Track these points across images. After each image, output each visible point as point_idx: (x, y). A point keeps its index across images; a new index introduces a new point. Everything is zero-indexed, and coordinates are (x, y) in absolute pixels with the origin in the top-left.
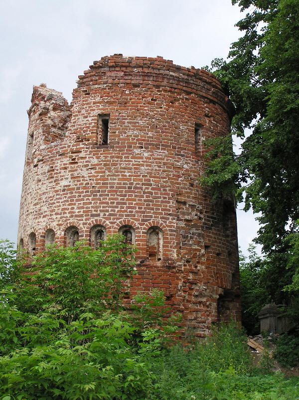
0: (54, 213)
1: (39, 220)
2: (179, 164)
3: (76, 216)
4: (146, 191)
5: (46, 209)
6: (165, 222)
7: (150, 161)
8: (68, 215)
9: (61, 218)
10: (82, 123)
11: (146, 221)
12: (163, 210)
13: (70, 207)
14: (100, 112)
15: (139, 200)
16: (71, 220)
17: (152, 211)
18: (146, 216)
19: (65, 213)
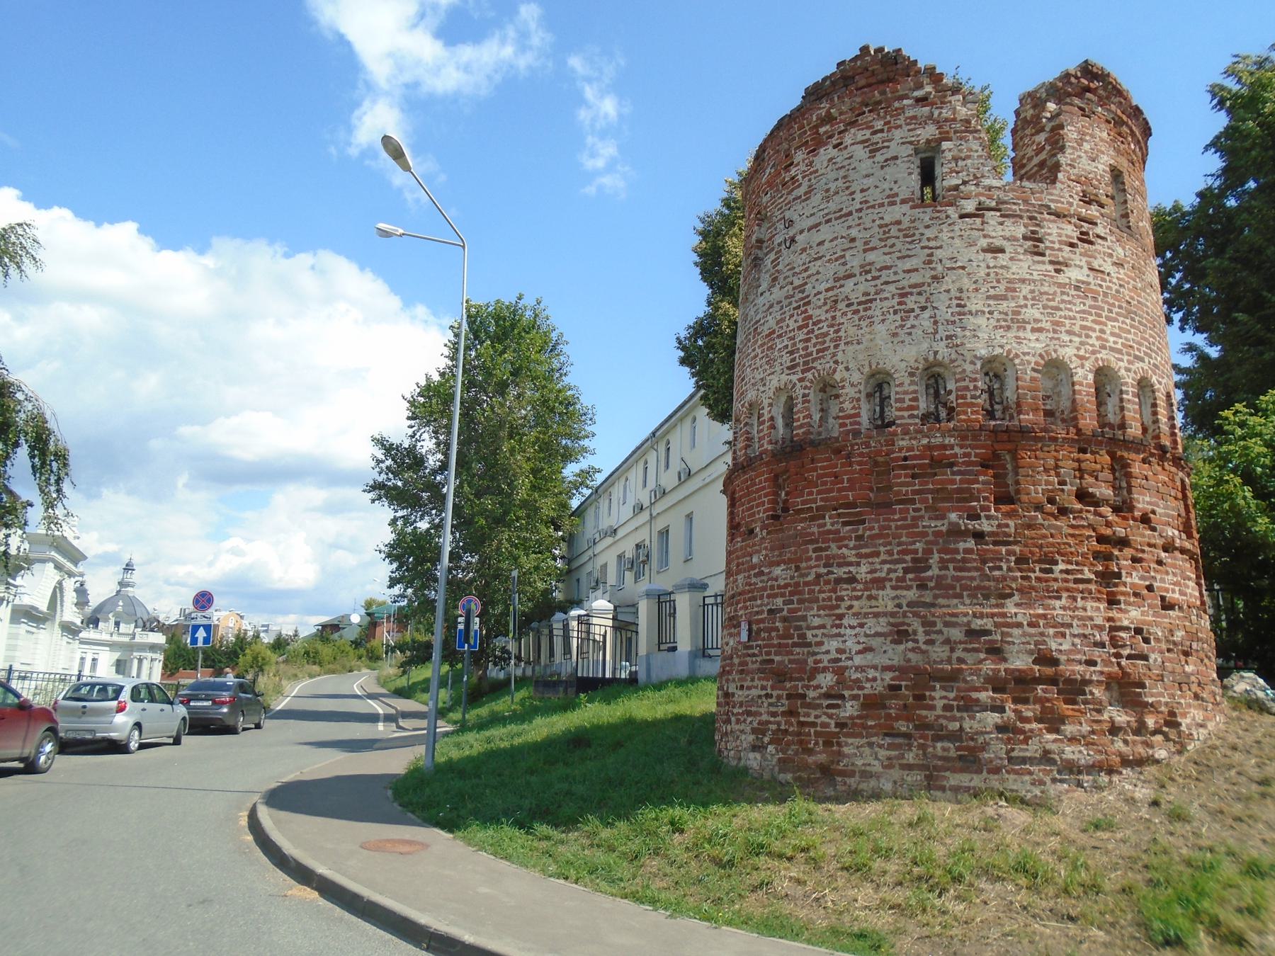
0: (1063, 329)
1: (1021, 334)
3: (1112, 349)
5: (1038, 316)
8: (1097, 343)
9: (1082, 343)
10: (1088, 168)
13: (1097, 327)
14: (1112, 162)
16: (1103, 354)
19: (1088, 336)
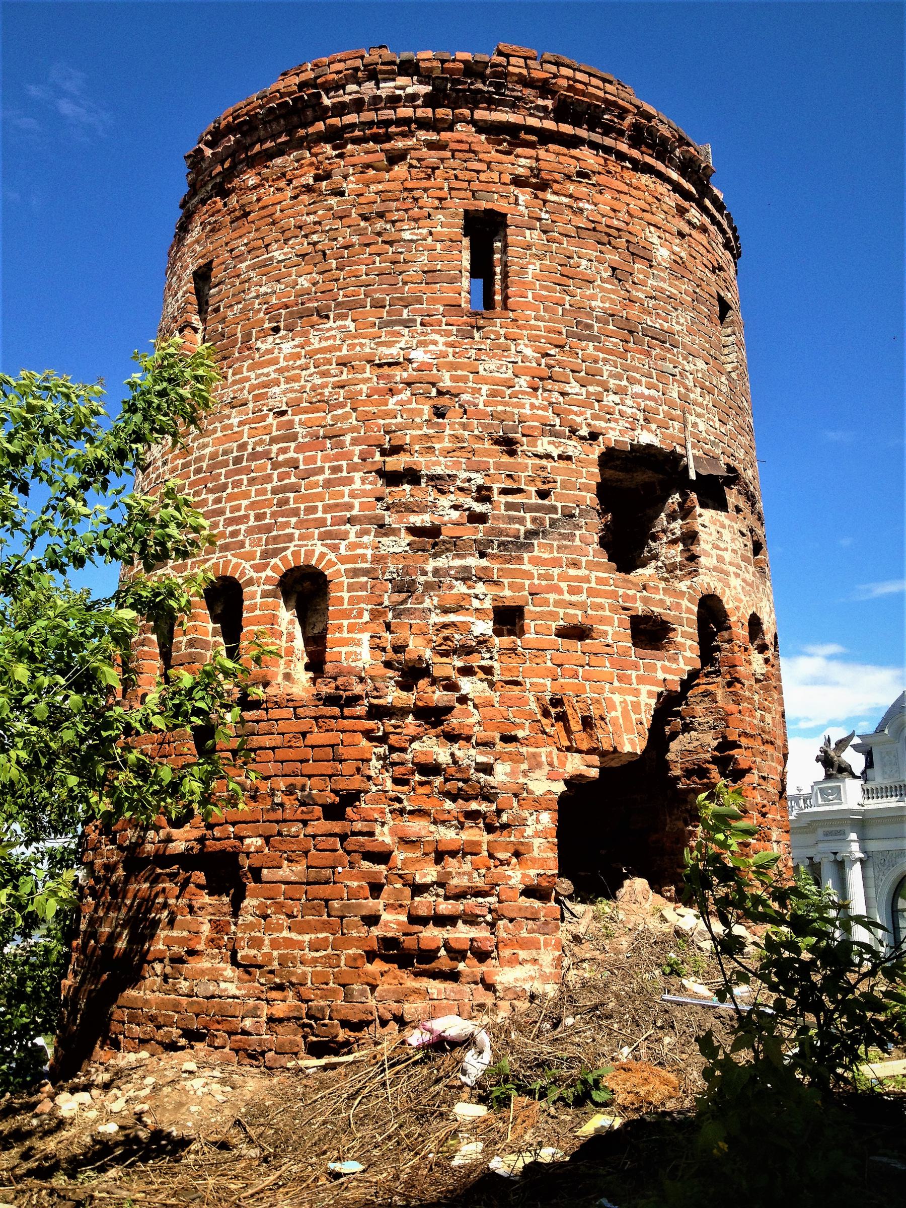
2: (394, 351)
4: (281, 458)
6: (335, 548)
7: (298, 363)
11: (275, 553)
12: (327, 509)
15: (258, 493)
17: (294, 520)
18: (275, 538)
